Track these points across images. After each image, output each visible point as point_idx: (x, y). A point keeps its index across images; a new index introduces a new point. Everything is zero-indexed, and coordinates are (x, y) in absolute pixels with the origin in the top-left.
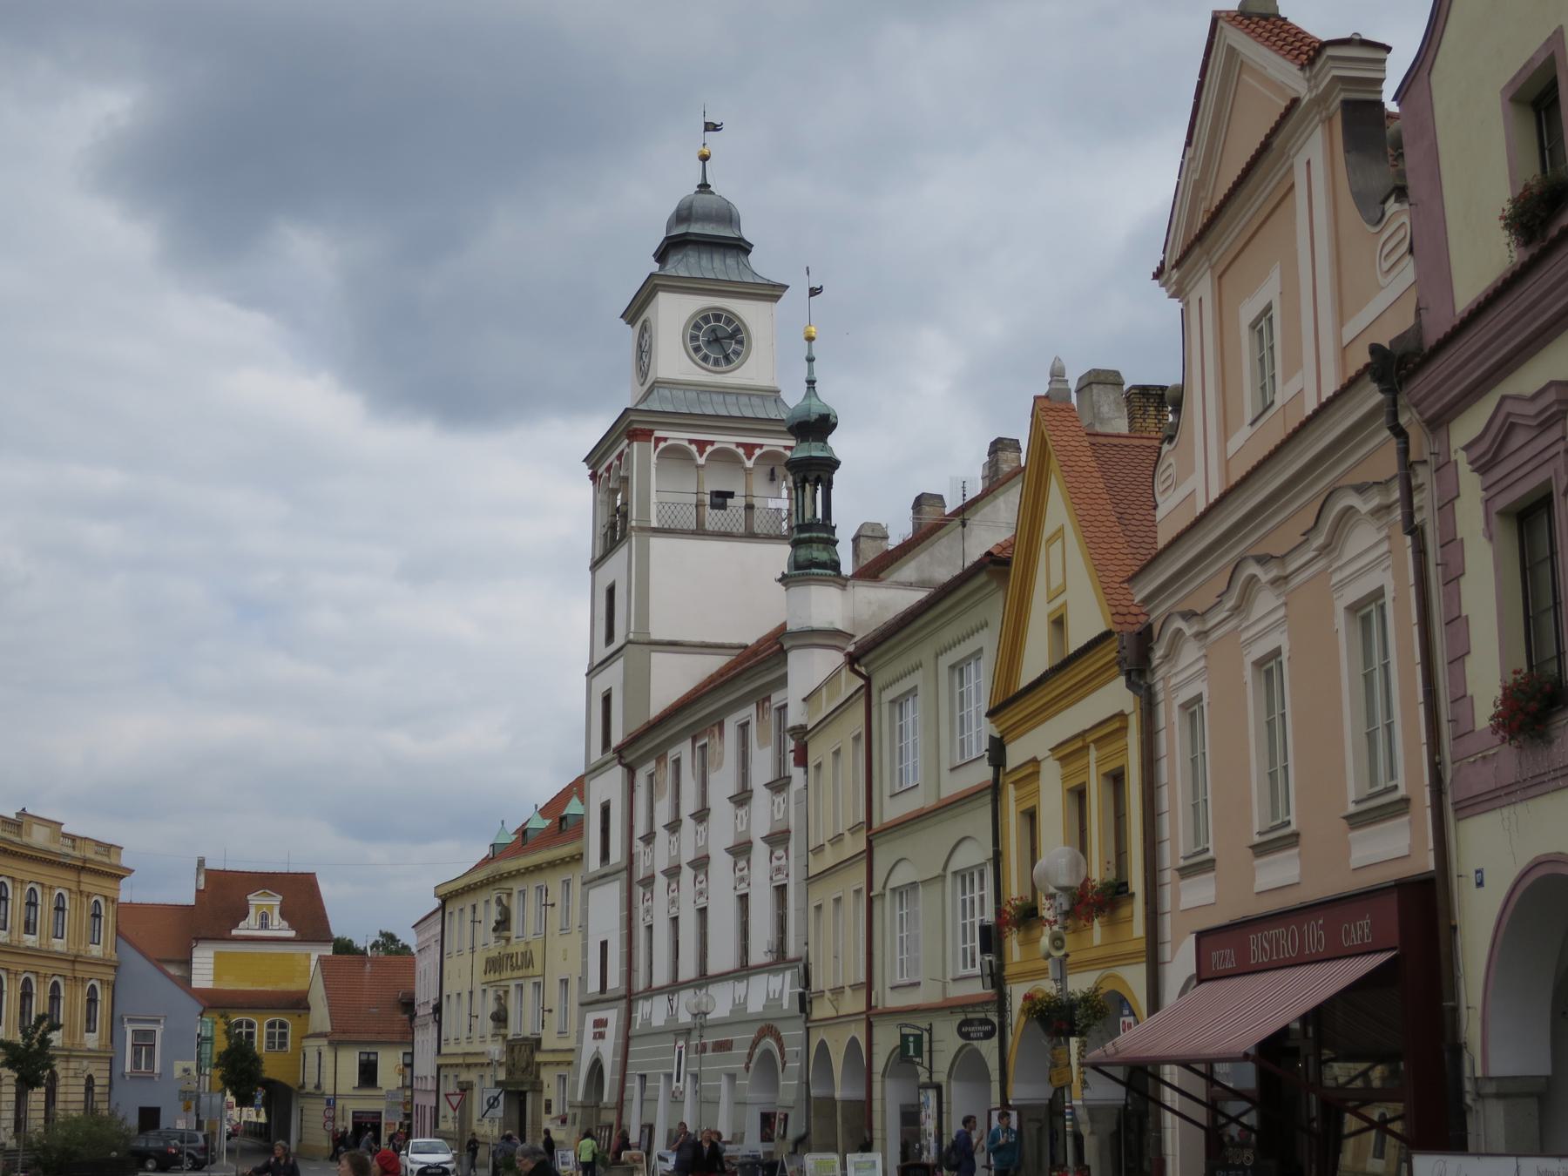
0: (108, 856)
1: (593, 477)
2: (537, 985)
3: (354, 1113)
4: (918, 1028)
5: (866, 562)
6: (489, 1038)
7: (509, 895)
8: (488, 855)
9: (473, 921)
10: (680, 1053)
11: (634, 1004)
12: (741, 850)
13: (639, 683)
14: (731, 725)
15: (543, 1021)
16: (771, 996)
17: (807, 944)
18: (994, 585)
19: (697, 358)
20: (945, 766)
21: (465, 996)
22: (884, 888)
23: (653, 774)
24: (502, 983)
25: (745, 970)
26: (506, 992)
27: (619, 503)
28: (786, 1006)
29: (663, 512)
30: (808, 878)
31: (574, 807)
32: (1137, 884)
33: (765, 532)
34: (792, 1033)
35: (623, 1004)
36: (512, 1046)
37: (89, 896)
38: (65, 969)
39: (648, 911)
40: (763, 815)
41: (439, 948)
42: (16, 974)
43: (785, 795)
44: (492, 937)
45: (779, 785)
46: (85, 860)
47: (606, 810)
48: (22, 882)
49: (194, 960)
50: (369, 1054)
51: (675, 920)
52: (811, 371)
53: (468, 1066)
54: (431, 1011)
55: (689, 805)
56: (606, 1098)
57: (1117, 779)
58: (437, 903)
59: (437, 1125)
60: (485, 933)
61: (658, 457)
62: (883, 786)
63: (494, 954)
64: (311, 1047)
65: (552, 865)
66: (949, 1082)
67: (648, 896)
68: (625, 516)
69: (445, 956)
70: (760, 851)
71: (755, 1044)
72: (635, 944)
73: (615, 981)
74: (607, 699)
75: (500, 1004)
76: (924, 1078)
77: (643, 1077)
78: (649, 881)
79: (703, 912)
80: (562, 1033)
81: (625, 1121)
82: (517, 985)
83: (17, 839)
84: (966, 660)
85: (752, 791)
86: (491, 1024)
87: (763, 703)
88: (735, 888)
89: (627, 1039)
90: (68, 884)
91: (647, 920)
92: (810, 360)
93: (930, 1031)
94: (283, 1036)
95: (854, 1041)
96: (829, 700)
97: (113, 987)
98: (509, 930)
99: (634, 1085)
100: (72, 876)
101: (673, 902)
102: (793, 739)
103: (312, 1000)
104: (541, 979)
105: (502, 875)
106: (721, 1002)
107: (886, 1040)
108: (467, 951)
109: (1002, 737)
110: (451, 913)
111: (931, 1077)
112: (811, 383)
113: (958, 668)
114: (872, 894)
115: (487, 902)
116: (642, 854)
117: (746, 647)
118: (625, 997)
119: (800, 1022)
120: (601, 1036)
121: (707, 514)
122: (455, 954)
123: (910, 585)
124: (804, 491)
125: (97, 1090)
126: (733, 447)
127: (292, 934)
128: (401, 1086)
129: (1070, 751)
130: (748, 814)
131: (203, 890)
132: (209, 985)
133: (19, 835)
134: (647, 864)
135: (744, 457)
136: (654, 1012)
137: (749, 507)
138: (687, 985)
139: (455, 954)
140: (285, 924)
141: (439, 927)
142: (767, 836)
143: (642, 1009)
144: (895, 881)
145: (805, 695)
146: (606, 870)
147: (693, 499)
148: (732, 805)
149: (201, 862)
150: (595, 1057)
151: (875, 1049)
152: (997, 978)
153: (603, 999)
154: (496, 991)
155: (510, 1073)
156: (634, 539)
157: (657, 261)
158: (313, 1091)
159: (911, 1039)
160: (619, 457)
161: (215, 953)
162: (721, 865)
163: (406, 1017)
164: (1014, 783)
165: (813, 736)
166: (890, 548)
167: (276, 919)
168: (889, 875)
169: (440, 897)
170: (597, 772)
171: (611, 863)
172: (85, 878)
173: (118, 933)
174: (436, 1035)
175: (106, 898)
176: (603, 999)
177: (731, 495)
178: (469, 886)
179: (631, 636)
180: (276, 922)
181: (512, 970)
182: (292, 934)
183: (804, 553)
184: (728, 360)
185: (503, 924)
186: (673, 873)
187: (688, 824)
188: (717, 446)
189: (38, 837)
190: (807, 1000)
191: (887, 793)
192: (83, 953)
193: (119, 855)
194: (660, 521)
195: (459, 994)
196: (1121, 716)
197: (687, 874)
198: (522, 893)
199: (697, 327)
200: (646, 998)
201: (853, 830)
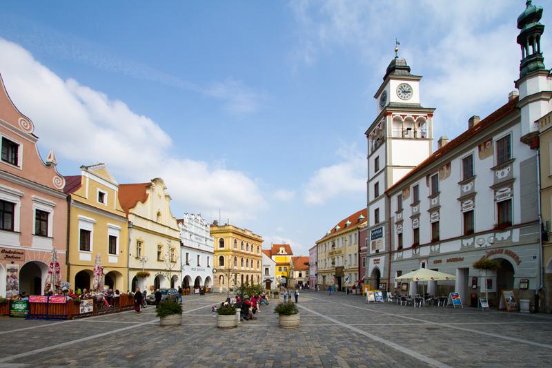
43: (509, 167)
47: (377, 211)
65: (346, 233)
78: (400, 222)
86: (331, 265)
88: (462, 211)
185: (333, 246)
186: (416, 216)
189: (248, 234)
198: (338, 240)
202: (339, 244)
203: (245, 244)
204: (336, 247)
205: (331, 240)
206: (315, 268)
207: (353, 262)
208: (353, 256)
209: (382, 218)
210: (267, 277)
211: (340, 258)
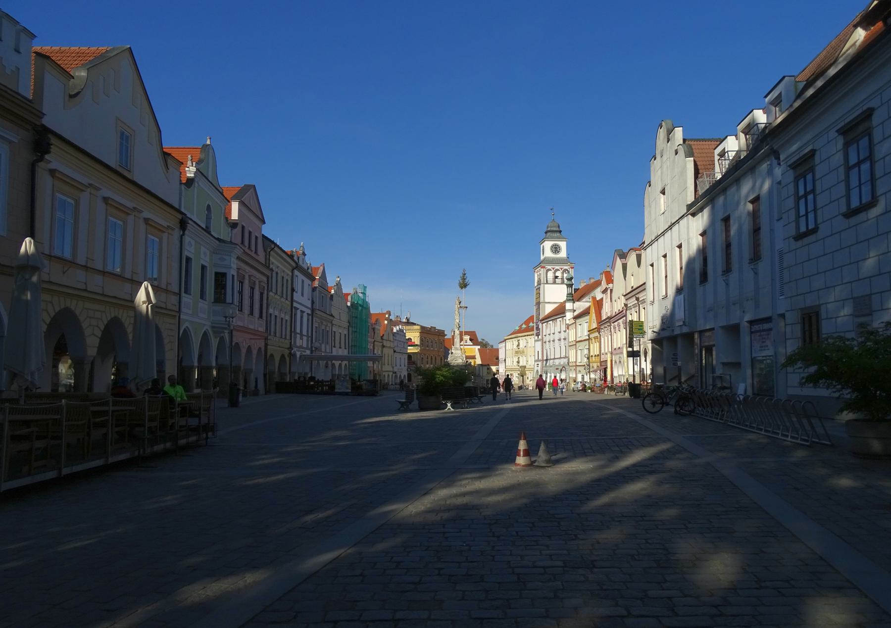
25: (561, 358)
40: (563, 335)
60: (515, 347)
70: (562, 340)
73: (540, 358)
78: (545, 342)
127: (472, 344)
129: (595, 338)
138: (552, 359)
153: (538, 360)
162: (556, 341)
163: (497, 360)
167: (468, 341)
176: (538, 360)
181: (521, 353)
182: (472, 344)
185: (518, 345)
186: (549, 342)
187: (552, 335)
189: (433, 330)
202: (523, 342)
204: (521, 346)
206: (504, 364)
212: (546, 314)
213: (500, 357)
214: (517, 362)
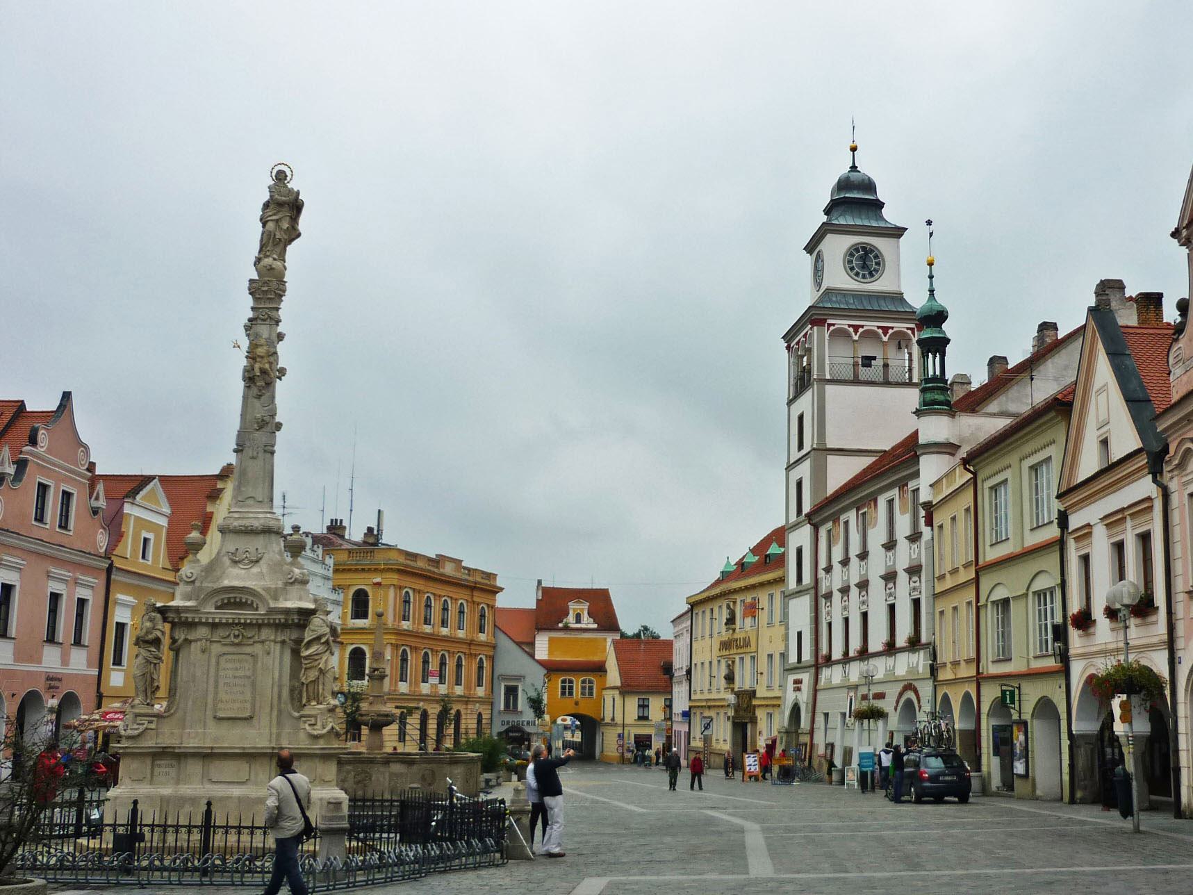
0: (489, 580)
1: (788, 348)
2: (753, 658)
3: (635, 735)
4: (1012, 686)
5: (958, 398)
6: (722, 689)
7: (735, 603)
8: (719, 578)
9: (712, 619)
10: (851, 700)
11: (820, 670)
12: (890, 577)
13: (819, 474)
14: (882, 501)
15: (757, 680)
16: (911, 666)
17: (934, 634)
18: (1060, 418)
19: (852, 274)
20: (1027, 527)
21: (707, 665)
22: (987, 601)
23: (831, 530)
24: (731, 657)
25: (891, 648)
26: (733, 662)
27: (805, 364)
28: (921, 670)
29: (833, 369)
30: (934, 595)
31: (774, 549)
32: (1160, 599)
33: (896, 381)
34: (926, 689)
35: (813, 670)
36: (738, 694)
37: (478, 604)
38: (465, 649)
39: (828, 613)
40: (904, 555)
41: (689, 635)
42: (437, 651)
43: (918, 543)
44: (724, 628)
45: (915, 537)
46: (475, 583)
47: (799, 551)
48: (440, 596)
49: (536, 642)
50: (644, 699)
51: (847, 620)
52: (931, 284)
53: (709, 707)
54: (685, 673)
55: (855, 549)
56: (802, 726)
57: (1145, 538)
58: (686, 607)
59: (689, 743)
61: (829, 336)
62: (987, 537)
63: (725, 638)
64: (608, 696)
65: (762, 585)
66: (1032, 722)
67: (828, 604)
68: (809, 372)
69: (693, 642)
70: (902, 577)
71: (901, 694)
72: (820, 633)
73: (807, 656)
74: (799, 484)
75: (730, 669)
76: (1015, 717)
77: (826, 715)
78: (829, 596)
79: (865, 616)
80: (769, 687)
81: (815, 741)
82: (740, 658)
83: (436, 570)
84: (1040, 464)
85: (896, 541)
86: (723, 682)
87: (903, 487)
88: (886, 600)
89: (816, 691)
90: (466, 597)
91: (827, 618)
92: (931, 277)
93: (1019, 688)
94: (591, 688)
95: (967, 696)
96: (947, 487)
97: (492, 659)
98: (735, 624)
99: (820, 719)
100: (468, 592)
101: (845, 608)
102: (924, 510)
103: (608, 666)
104: (755, 654)
105: (730, 590)
106: (880, 667)
107: (990, 694)
108: (707, 636)
109: (1066, 510)
110: (697, 614)
111: (1020, 716)
112: (932, 291)
113: (1035, 468)
114: (979, 604)
115: (720, 607)
116: (824, 578)
117: (885, 451)
118: (814, 666)
119: (930, 683)
120: (799, 689)
121: (860, 370)
122: (699, 638)
123: (994, 415)
124: (928, 358)
125: (484, 721)
126: (876, 329)
127: (595, 626)
128: (663, 718)
129: (1114, 520)
130: (894, 555)
131: (541, 600)
132: (546, 657)
133: (438, 567)
134: (827, 585)
135: (882, 335)
136: (833, 675)
137: (886, 366)
138: (854, 659)
139: (699, 638)
140: (592, 620)
141: (690, 621)
142: (907, 568)
143: (825, 673)
144: (994, 597)
145: (931, 483)
146: (800, 588)
147: (851, 361)
148: (883, 549)
149: (539, 582)
150: (795, 701)
151: (982, 699)
152: (1064, 657)
153: (799, 667)
154: (727, 661)
155: (736, 711)
156: (815, 386)
157: (825, 214)
158: (610, 722)
159: (1008, 693)
160: (805, 336)
161: (549, 638)
162: (877, 585)
163: (668, 676)
164: (1074, 538)
165: (937, 508)
166: (973, 389)
167: (585, 618)
168: (990, 593)
169: (690, 604)
170: (794, 528)
171: (803, 584)
172: (476, 593)
173: (495, 625)
174: (688, 688)
175: (488, 605)
176: (799, 667)
177: (874, 358)
178: (709, 597)
179: (815, 446)
180: (585, 619)
181: (738, 647)
182: (595, 626)
183: (929, 396)
184: (872, 275)
185: (731, 621)
186: (845, 591)
187: (854, 561)
188: (865, 328)
189: (448, 570)
190: (935, 668)
191: (988, 543)
192: (475, 638)
193: (495, 579)
194: (831, 375)
195: (702, 663)
196: (1149, 499)
197: (854, 591)
199: (852, 255)
200: (828, 666)
201: (966, 566)
203: (436, 606)
205: (724, 603)
206: (685, 687)
207: (776, 684)
208: (777, 658)
209: (807, 579)
210: (512, 718)
211: (747, 659)
212: (830, 490)
213: (676, 665)
214: (725, 678)
